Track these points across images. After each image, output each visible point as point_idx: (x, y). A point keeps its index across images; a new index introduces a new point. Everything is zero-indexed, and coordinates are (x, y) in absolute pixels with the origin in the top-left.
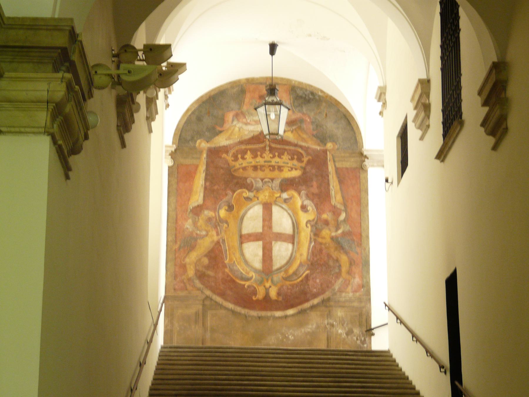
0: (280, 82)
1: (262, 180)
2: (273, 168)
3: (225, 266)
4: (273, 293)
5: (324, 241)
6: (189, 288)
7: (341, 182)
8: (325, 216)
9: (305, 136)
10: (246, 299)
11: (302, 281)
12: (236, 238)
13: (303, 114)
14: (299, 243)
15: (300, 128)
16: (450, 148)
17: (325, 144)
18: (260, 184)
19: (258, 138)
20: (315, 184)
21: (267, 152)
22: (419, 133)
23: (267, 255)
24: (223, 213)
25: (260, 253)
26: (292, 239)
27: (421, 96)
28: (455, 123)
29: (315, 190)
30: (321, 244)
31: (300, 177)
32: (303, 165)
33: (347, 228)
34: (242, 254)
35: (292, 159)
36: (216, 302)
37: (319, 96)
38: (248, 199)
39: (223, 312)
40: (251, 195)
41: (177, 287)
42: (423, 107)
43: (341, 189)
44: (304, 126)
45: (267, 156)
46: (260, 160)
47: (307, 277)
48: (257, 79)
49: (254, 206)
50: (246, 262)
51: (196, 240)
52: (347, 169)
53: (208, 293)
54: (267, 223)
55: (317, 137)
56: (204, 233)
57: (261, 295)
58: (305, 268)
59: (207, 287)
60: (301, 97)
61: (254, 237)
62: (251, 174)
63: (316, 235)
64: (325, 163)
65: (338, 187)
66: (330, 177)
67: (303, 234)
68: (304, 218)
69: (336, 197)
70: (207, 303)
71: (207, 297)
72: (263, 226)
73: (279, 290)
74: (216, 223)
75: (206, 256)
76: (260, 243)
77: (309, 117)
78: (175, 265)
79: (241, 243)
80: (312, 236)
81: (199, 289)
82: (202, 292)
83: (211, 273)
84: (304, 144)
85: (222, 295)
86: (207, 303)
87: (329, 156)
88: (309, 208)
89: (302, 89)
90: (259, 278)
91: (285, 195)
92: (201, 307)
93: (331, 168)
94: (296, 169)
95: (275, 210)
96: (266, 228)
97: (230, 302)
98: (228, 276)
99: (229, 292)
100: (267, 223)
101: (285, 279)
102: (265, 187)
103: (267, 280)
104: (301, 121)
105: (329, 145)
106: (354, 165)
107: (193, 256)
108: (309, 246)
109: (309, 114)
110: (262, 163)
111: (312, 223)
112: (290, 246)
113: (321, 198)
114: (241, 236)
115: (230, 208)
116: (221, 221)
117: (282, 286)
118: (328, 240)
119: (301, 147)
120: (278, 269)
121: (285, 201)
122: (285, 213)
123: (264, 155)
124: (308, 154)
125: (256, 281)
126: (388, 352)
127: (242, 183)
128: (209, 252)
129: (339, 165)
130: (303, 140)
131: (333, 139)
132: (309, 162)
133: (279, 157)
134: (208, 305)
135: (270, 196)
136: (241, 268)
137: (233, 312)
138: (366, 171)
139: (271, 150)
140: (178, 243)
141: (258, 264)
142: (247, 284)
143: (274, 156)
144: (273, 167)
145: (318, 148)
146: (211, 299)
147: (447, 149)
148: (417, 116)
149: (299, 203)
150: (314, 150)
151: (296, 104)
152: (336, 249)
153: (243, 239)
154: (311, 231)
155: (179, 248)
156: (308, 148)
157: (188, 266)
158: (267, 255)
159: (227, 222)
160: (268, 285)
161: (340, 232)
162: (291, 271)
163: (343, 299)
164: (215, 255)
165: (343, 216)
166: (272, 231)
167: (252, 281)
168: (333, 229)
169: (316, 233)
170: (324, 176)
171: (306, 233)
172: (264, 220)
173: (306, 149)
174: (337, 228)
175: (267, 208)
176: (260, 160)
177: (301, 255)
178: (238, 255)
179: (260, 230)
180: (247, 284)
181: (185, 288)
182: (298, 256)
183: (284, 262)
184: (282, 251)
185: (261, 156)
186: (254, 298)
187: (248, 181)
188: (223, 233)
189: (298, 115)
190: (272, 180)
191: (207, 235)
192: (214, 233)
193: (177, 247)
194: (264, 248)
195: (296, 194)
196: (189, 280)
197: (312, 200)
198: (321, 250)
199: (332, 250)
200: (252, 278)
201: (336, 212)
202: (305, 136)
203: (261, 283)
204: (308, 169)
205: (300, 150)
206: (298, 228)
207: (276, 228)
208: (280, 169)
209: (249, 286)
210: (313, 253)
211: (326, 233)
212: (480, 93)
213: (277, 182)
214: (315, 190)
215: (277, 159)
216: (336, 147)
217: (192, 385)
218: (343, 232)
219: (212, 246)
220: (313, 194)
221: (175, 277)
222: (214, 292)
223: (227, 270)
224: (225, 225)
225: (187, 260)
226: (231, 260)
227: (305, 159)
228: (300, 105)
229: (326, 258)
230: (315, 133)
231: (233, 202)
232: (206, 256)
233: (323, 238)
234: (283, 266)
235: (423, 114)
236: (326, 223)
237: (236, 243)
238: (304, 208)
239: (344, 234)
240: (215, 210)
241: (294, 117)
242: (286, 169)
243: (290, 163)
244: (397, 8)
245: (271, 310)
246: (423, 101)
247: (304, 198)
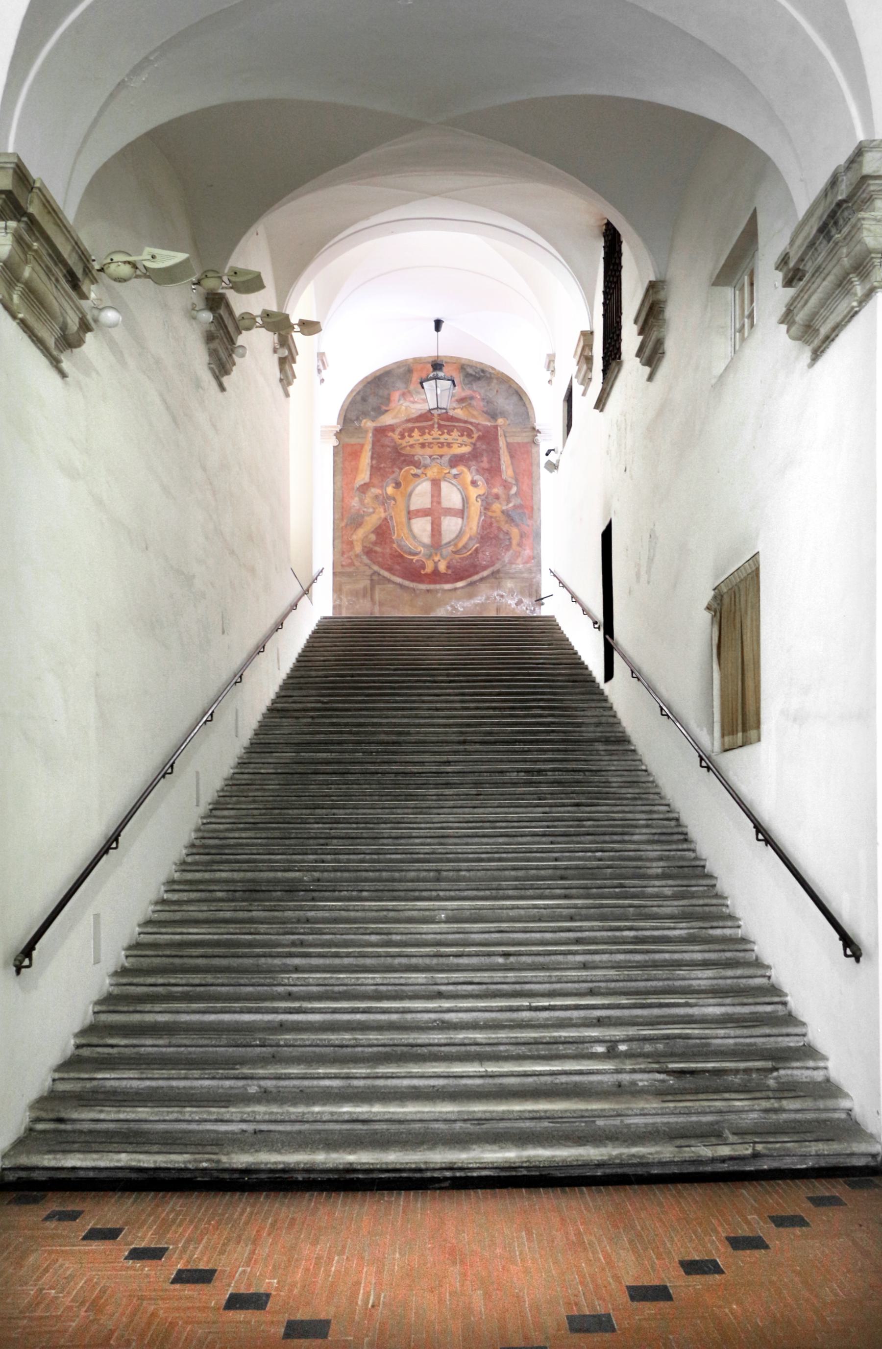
0: (449, 361)
1: (430, 457)
2: (441, 445)
3: (392, 542)
4: (442, 567)
5: (494, 515)
6: (357, 563)
7: (512, 457)
8: (495, 490)
9: (475, 413)
10: (414, 573)
11: (471, 554)
12: (404, 514)
13: (474, 391)
14: (468, 517)
15: (470, 404)
16: (609, 394)
17: (496, 420)
18: (428, 461)
19: (426, 416)
20: (485, 459)
21: (436, 430)
22: (582, 388)
23: (436, 530)
24: (390, 490)
25: (429, 528)
26: (461, 513)
27: (583, 349)
28: (614, 364)
29: (485, 465)
30: (491, 517)
31: (469, 453)
32: (473, 441)
33: (518, 501)
34: (411, 530)
35: (462, 435)
36: (384, 577)
37: (490, 373)
38: (416, 476)
39: (390, 586)
40: (419, 471)
41: (344, 563)
42: (586, 359)
43: (512, 464)
44: (474, 403)
45: (436, 433)
46: (428, 438)
47: (476, 550)
48: (425, 358)
49: (422, 482)
50: (414, 537)
51: (363, 517)
52: (518, 443)
53: (376, 568)
54: (435, 499)
55: (486, 413)
56: (371, 510)
57: (429, 569)
58: (474, 542)
59: (374, 563)
60: (471, 375)
61: (424, 513)
62: (418, 450)
63: (486, 509)
64: (496, 439)
65: (509, 462)
66: (501, 452)
67: (473, 509)
68: (473, 492)
69: (507, 471)
70: (375, 578)
71: (375, 573)
72: (432, 502)
73: (449, 563)
74: (384, 500)
75: (373, 532)
76: (429, 518)
77: (480, 394)
78: (343, 542)
79: (410, 519)
80: (483, 511)
81: (366, 565)
82: (370, 568)
83: (378, 549)
84: (473, 420)
85: (390, 570)
86: (375, 578)
87: (500, 432)
88: (479, 483)
89: (471, 367)
90: (428, 552)
91: (454, 471)
92: (369, 582)
93: (502, 443)
94: (466, 445)
95: (444, 486)
96: (435, 504)
97: (398, 576)
98: (396, 551)
99: (398, 567)
100: (435, 499)
101: (455, 553)
102: (434, 464)
103: (436, 554)
104: (472, 398)
105: (500, 421)
106: (526, 440)
107: (360, 533)
108: (479, 520)
109: (479, 391)
110: (432, 441)
111: (483, 497)
112: (460, 521)
113: (492, 472)
114: (409, 512)
115: (398, 485)
116: (389, 498)
117: (451, 560)
118: (499, 514)
119: (471, 423)
120: (446, 544)
121: (455, 476)
122: (455, 488)
123: (433, 432)
124: (478, 430)
125: (424, 555)
126: (553, 617)
127: (411, 461)
128: (376, 529)
129: (510, 440)
130: (474, 416)
131: (503, 414)
132: (479, 438)
133: (449, 433)
134: (375, 580)
135: (438, 472)
136: (410, 544)
137: (401, 586)
138: (538, 445)
139: (440, 427)
140: (345, 521)
141: (426, 539)
142: (415, 558)
143: (443, 433)
144: (442, 443)
145: (489, 424)
146: (379, 574)
147: (605, 395)
148: (579, 370)
149: (468, 477)
150: (485, 427)
151: (466, 382)
152: (507, 522)
153: (411, 515)
154: (482, 505)
155: (346, 526)
156: (478, 424)
157: (355, 543)
158: (436, 530)
159: (394, 499)
160: (436, 559)
161: (511, 505)
162: (460, 545)
163: (512, 571)
164: (383, 532)
165: (514, 490)
166: (442, 506)
167: (421, 555)
168: (504, 503)
169: (487, 507)
170: (494, 453)
171: (476, 507)
172: (432, 496)
173: (476, 425)
174: (508, 502)
175: (436, 483)
176: (428, 438)
177: (471, 529)
178: (406, 530)
179: (429, 506)
180: (415, 558)
181: (352, 564)
182: (467, 530)
183: (453, 536)
184: (451, 526)
185: (429, 434)
186: (423, 572)
187: (416, 458)
188: (391, 510)
189: (468, 393)
190: (441, 456)
191: (374, 512)
192: (382, 510)
193: (343, 524)
194: (432, 524)
195: (465, 470)
196: (357, 556)
197: (482, 475)
198: (491, 524)
199: (503, 523)
200: (420, 552)
201: (506, 486)
202: (475, 413)
203: (430, 556)
204: (479, 444)
205: (470, 426)
206: (468, 503)
207: (445, 504)
208: (449, 445)
209: (417, 561)
210: (483, 526)
211: (497, 507)
212: (636, 322)
213: (446, 459)
214: (485, 465)
215: (446, 436)
216: (508, 422)
217: (343, 651)
218: (514, 506)
219: (379, 523)
220: (483, 469)
221: (343, 553)
222: (382, 567)
223: (395, 546)
224: (393, 502)
225: (354, 537)
226: (398, 535)
227: (475, 436)
228: (470, 383)
229: (496, 532)
230: (485, 409)
231: (400, 479)
232: (373, 532)
233: (494, 512)
234: (453, 540)
235: (585, 367)
236: (497, 497)
237: (404, 519)
238: (474, 483)
239: (515, 507)
240: (382, 487)
241: (463, 394)
242: (455, 446)
243: (460, 440)
244: (555, 257)
245: (440, 583)
246: (586, 354)
247: (474, 473)
